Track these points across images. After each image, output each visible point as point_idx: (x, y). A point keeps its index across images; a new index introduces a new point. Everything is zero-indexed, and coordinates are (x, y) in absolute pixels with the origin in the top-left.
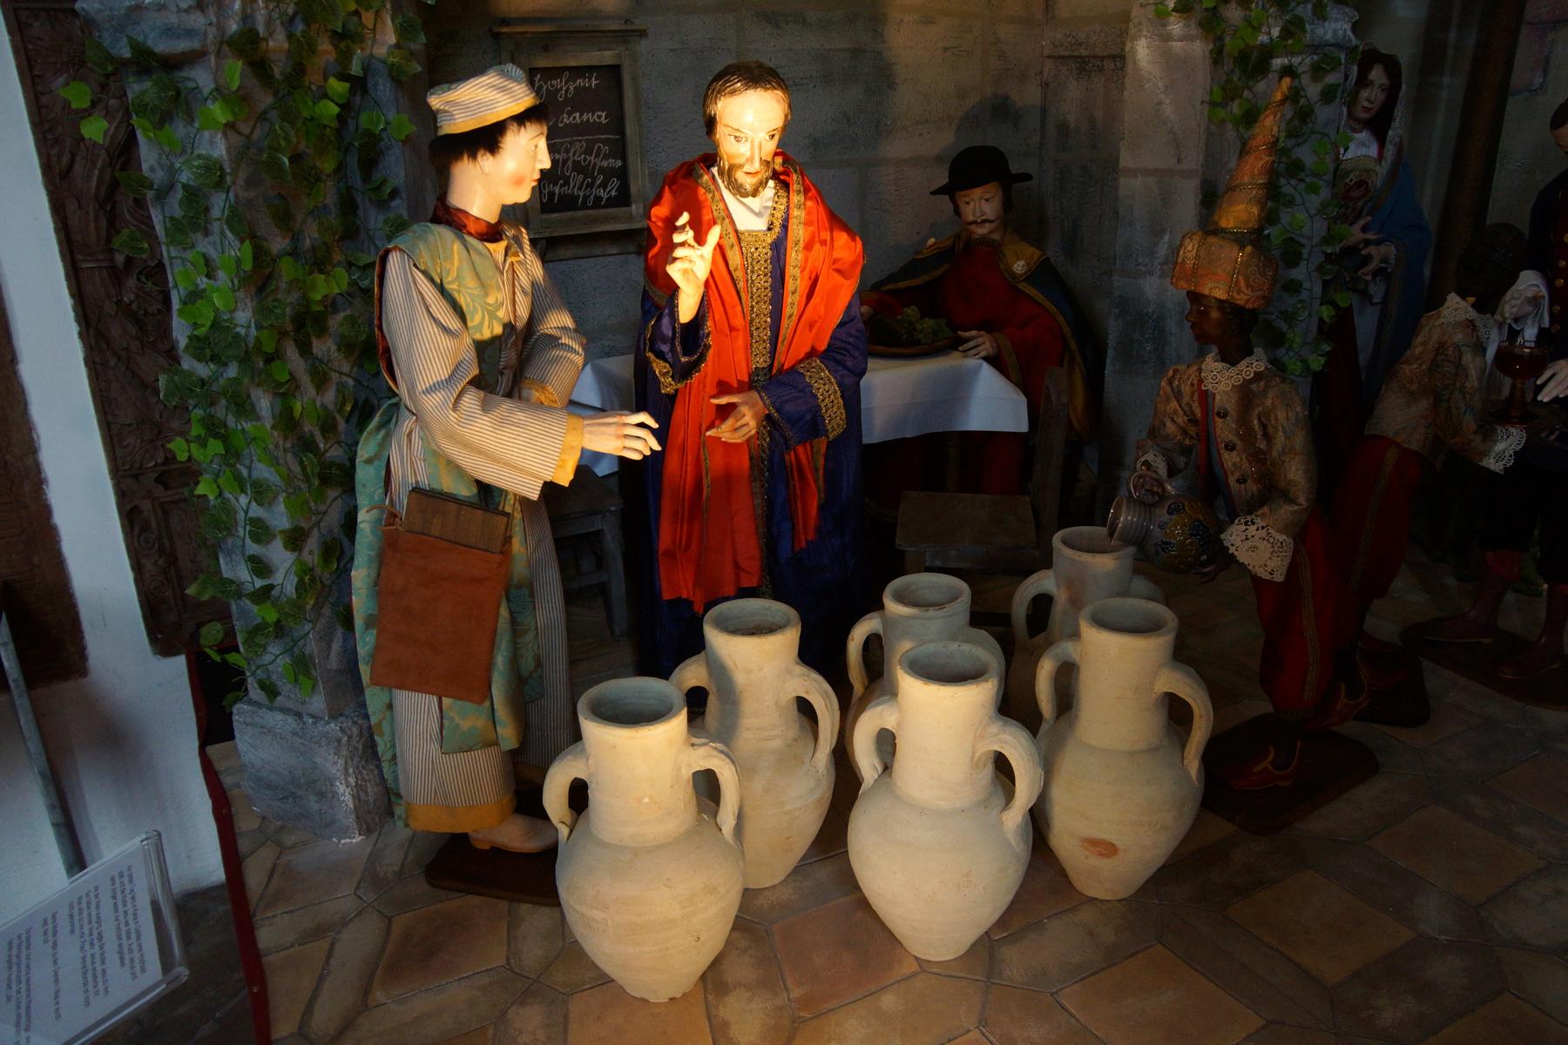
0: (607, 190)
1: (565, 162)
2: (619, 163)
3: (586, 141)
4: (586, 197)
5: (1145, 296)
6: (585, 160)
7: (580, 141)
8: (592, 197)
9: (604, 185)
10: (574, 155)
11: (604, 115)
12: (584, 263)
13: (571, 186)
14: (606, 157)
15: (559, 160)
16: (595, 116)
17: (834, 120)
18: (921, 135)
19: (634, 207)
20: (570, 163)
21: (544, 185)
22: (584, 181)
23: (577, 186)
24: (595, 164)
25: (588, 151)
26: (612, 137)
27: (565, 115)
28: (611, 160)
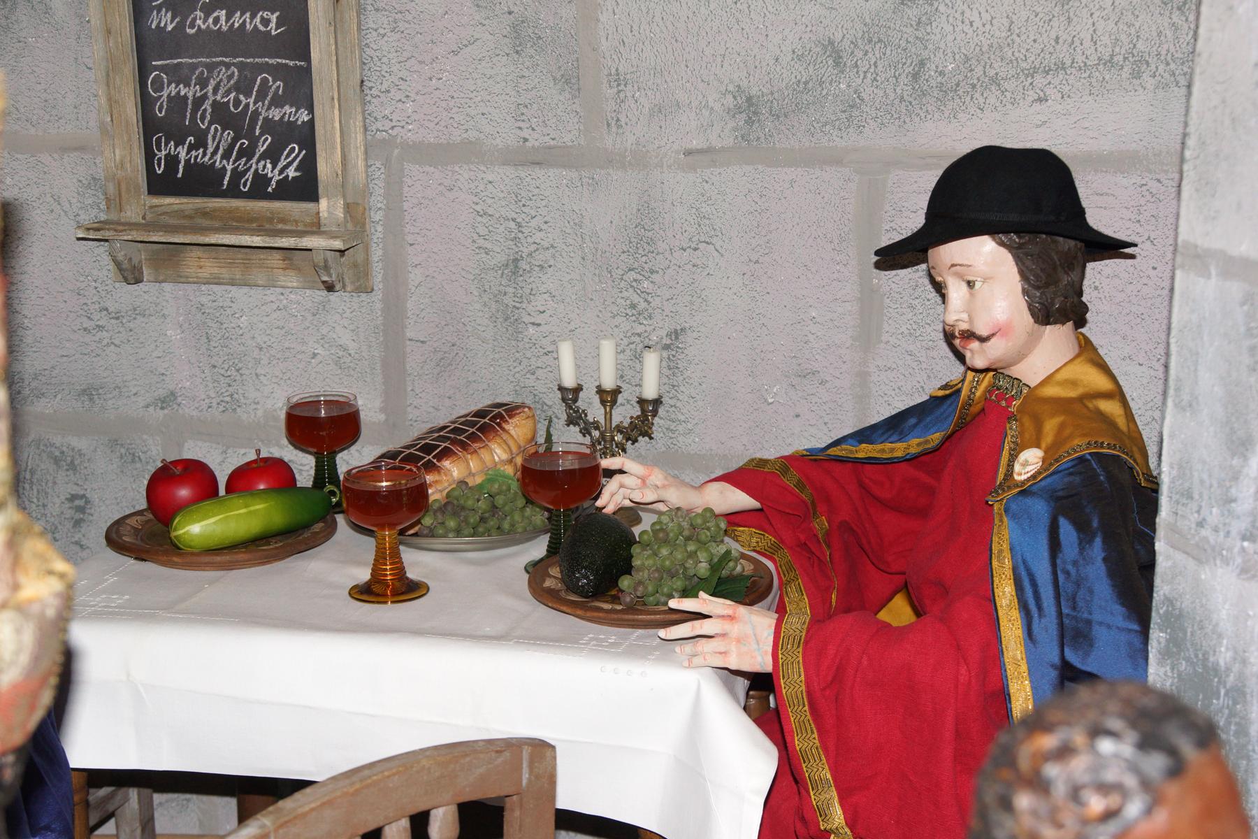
0: (280, 166)
1: (199, 102)
2: (304, 116)
3: (241, 67)
4: (237, 175)
5: (1215, 616)
6: (237, 103)
7: (228, 66)
8: (250, 175)
9: (273, 155)
10: (215, 91)
11: (274, 18)
12: (235, 291)
13: (210, 150)
14: (277, 102)
15: (186, 98)
16: (258, 19)
17: (800, 58)
18: (1040, 100)
19: (323, 203)
20: (207, 105)
21: (159, 141)
22: (235, 140)
23: (221, 152)
24: (256, 113)
25: (243, 87)
26: (291, 63)
27: (198, 13)
28: (287, 109)
